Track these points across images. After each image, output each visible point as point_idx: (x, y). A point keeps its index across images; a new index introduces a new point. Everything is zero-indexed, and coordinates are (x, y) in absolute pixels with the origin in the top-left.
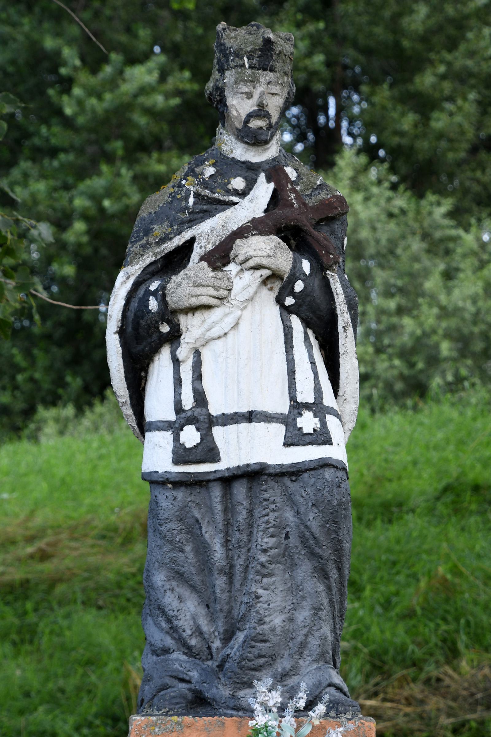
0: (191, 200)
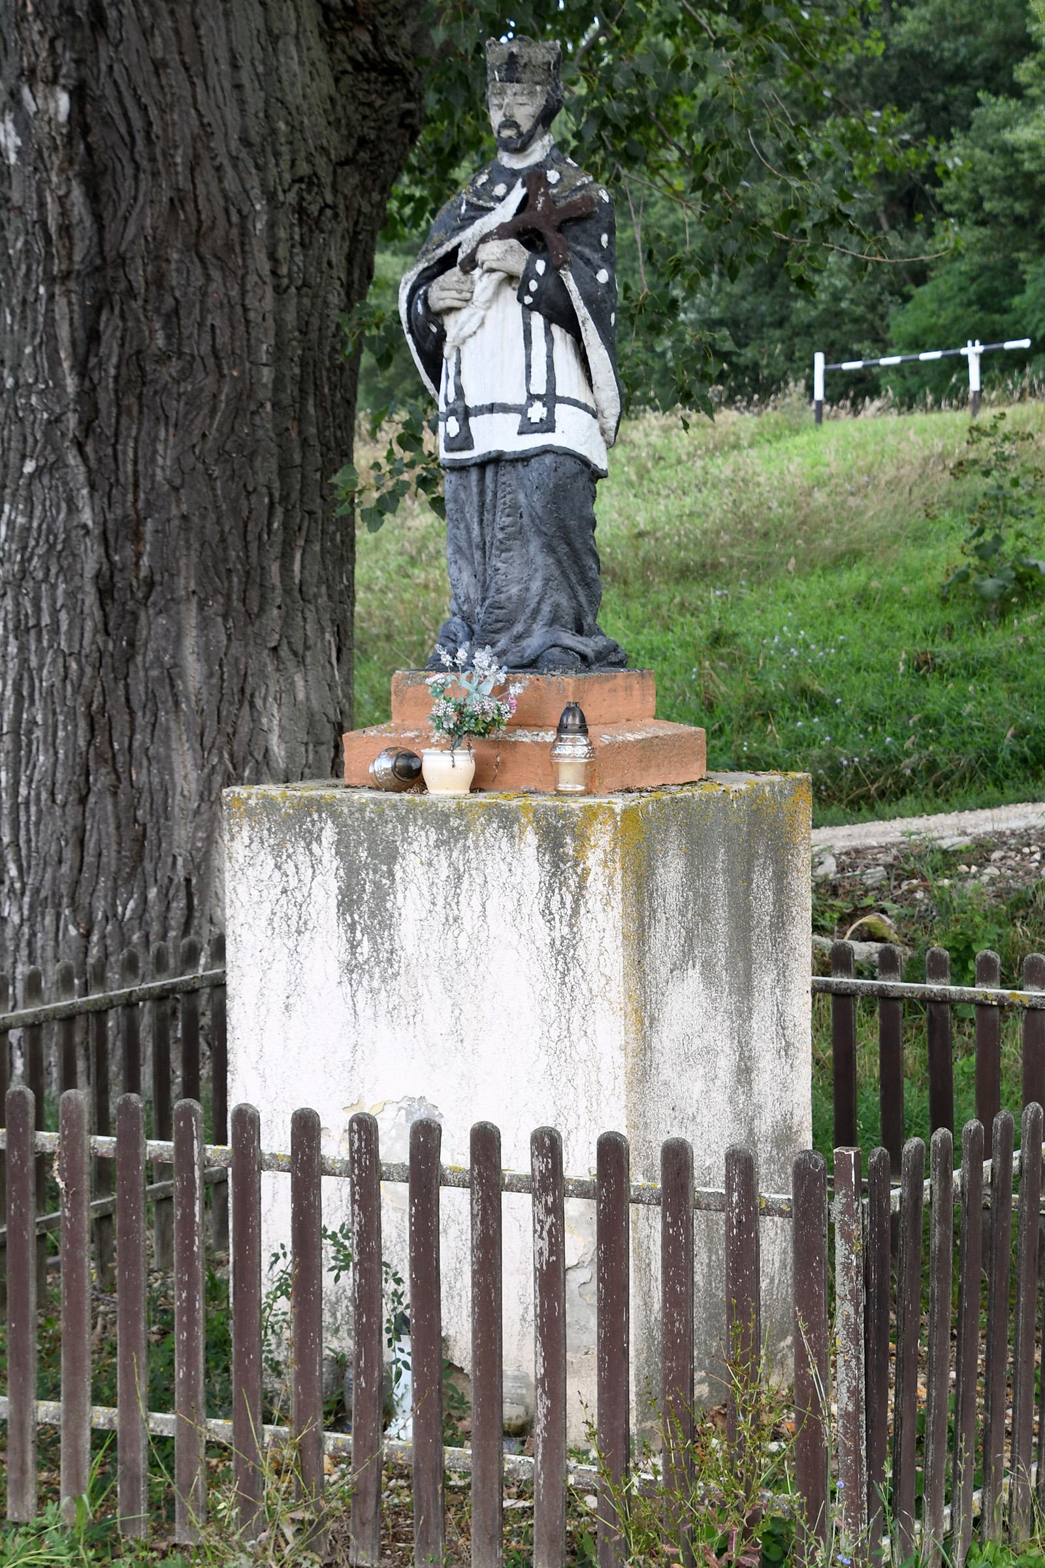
0: (464, 208)
